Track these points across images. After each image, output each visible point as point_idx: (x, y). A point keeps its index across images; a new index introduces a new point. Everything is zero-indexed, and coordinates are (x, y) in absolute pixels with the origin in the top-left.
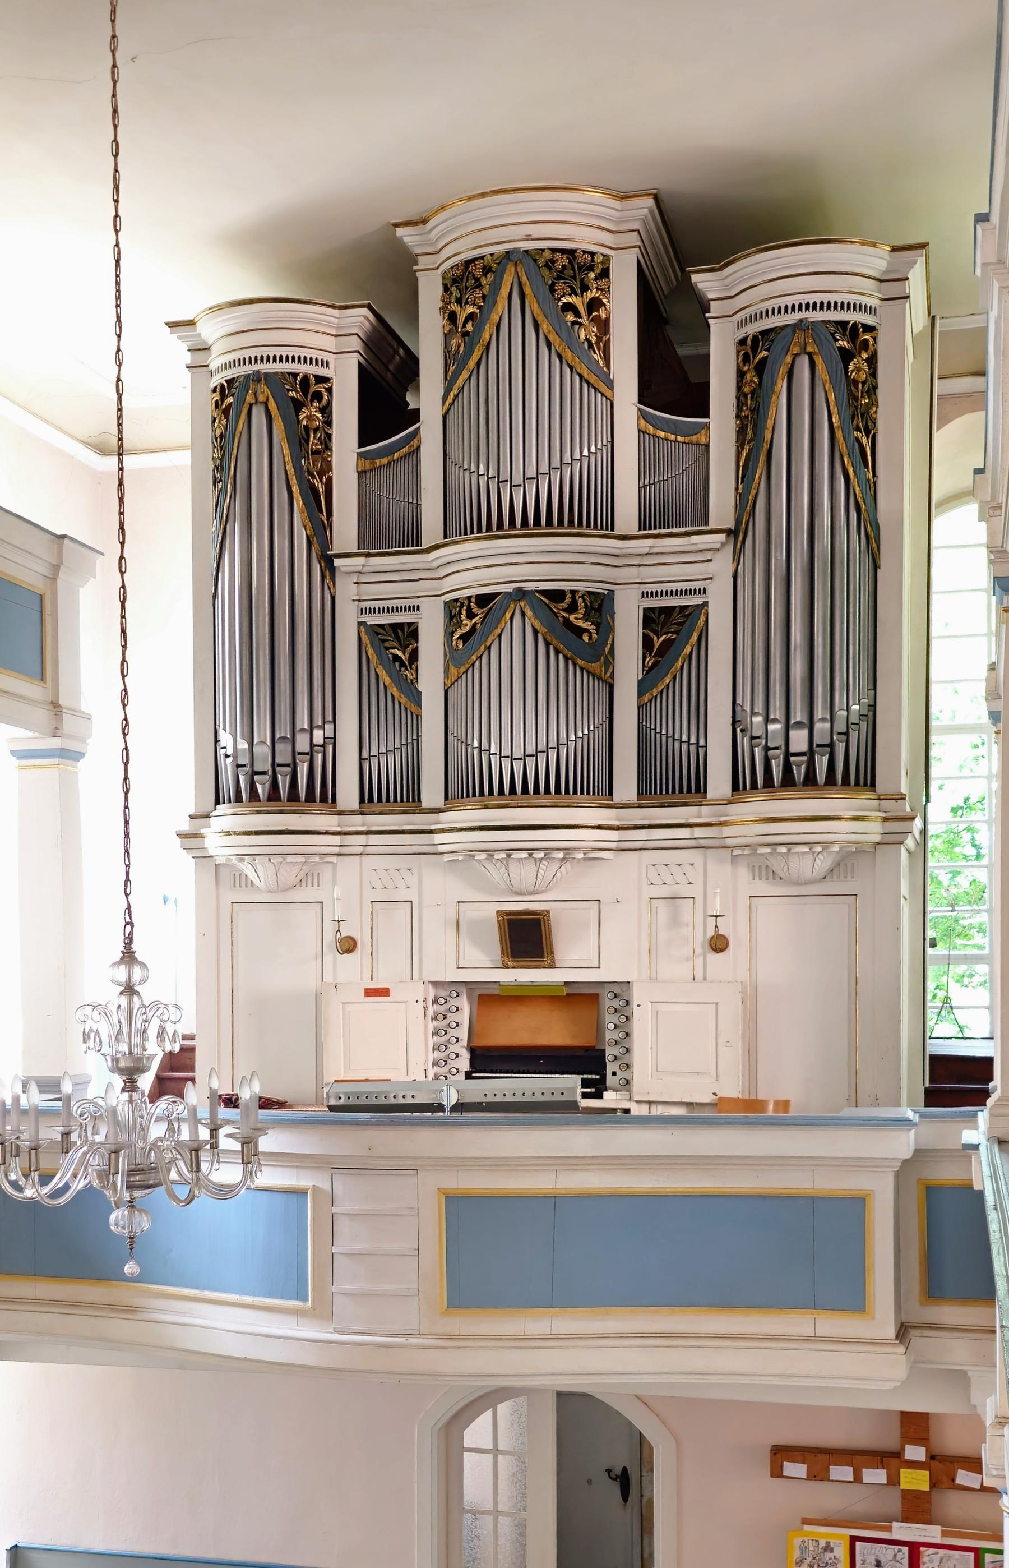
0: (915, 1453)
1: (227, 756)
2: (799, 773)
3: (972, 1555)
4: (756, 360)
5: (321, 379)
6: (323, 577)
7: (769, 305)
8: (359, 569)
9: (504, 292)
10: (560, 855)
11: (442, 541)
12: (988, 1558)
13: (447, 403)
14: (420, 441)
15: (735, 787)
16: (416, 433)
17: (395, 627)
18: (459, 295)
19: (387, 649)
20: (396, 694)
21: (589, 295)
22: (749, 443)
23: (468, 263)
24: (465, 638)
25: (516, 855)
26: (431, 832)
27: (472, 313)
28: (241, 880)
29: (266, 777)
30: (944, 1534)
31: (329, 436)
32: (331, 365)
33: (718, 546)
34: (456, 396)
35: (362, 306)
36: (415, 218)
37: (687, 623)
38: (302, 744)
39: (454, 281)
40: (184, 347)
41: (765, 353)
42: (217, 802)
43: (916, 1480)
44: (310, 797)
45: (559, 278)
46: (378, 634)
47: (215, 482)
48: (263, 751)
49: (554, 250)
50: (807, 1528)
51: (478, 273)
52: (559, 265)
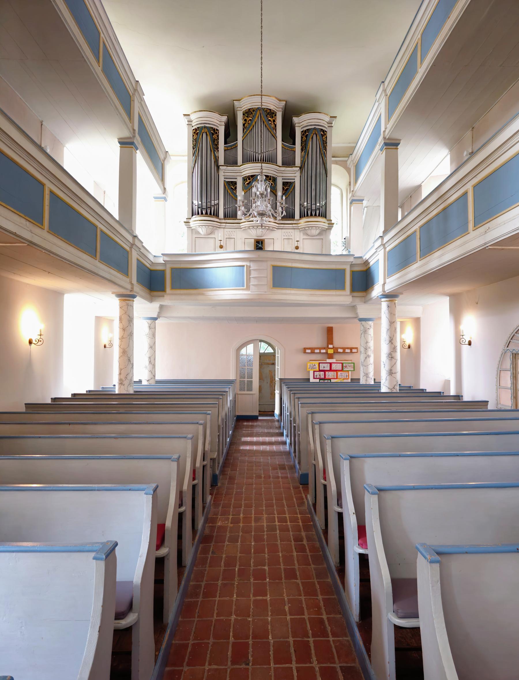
0: (331, 346)
1: (196, 206)
2: (314, 213)
3: (341, 364)
4: (306, 135)
5: (217, 130)
6: (217, 170)
7: (308, 124)
8: (225, 169)
9: (257, 116)
10: (268, 228)
11: (242, 164)
12: (344, 364)
13: (244, 137)
14: (237, 145)
15: (300, 217)
16: (237, 143)
17: (232, 182)
18: (247, 116)
19: (230, 186)
20: (232, 195)
21: (274, 119)
22: (304, 150)
23: (249, 109)
24: (248, 184)
25: (259, 227)
26: (240, 223)
27: (251, 119)
28: (198, 233)
29: (205, 210)
30: (336, 361)
31: (218, 142)
32: (219, 127)
33: (298, 170)
34: (246, 136)
35: (226, 116)
36: (238, 99)
37: (291, 185)
38: (213, 204)
39: (246, 113)
40: (186, 120)
41: (308, 133)
42: (192, 216)
43: (330, 351)
44: (214, 215)
45: (268, 114)
46: (228, 183)
47: (194, 149)
48: (204, 204)
49: (267, 109)
50: (311, 362)
51: (252, 111)
52: (268, 112)
